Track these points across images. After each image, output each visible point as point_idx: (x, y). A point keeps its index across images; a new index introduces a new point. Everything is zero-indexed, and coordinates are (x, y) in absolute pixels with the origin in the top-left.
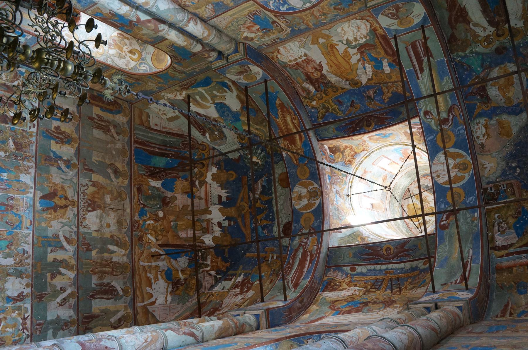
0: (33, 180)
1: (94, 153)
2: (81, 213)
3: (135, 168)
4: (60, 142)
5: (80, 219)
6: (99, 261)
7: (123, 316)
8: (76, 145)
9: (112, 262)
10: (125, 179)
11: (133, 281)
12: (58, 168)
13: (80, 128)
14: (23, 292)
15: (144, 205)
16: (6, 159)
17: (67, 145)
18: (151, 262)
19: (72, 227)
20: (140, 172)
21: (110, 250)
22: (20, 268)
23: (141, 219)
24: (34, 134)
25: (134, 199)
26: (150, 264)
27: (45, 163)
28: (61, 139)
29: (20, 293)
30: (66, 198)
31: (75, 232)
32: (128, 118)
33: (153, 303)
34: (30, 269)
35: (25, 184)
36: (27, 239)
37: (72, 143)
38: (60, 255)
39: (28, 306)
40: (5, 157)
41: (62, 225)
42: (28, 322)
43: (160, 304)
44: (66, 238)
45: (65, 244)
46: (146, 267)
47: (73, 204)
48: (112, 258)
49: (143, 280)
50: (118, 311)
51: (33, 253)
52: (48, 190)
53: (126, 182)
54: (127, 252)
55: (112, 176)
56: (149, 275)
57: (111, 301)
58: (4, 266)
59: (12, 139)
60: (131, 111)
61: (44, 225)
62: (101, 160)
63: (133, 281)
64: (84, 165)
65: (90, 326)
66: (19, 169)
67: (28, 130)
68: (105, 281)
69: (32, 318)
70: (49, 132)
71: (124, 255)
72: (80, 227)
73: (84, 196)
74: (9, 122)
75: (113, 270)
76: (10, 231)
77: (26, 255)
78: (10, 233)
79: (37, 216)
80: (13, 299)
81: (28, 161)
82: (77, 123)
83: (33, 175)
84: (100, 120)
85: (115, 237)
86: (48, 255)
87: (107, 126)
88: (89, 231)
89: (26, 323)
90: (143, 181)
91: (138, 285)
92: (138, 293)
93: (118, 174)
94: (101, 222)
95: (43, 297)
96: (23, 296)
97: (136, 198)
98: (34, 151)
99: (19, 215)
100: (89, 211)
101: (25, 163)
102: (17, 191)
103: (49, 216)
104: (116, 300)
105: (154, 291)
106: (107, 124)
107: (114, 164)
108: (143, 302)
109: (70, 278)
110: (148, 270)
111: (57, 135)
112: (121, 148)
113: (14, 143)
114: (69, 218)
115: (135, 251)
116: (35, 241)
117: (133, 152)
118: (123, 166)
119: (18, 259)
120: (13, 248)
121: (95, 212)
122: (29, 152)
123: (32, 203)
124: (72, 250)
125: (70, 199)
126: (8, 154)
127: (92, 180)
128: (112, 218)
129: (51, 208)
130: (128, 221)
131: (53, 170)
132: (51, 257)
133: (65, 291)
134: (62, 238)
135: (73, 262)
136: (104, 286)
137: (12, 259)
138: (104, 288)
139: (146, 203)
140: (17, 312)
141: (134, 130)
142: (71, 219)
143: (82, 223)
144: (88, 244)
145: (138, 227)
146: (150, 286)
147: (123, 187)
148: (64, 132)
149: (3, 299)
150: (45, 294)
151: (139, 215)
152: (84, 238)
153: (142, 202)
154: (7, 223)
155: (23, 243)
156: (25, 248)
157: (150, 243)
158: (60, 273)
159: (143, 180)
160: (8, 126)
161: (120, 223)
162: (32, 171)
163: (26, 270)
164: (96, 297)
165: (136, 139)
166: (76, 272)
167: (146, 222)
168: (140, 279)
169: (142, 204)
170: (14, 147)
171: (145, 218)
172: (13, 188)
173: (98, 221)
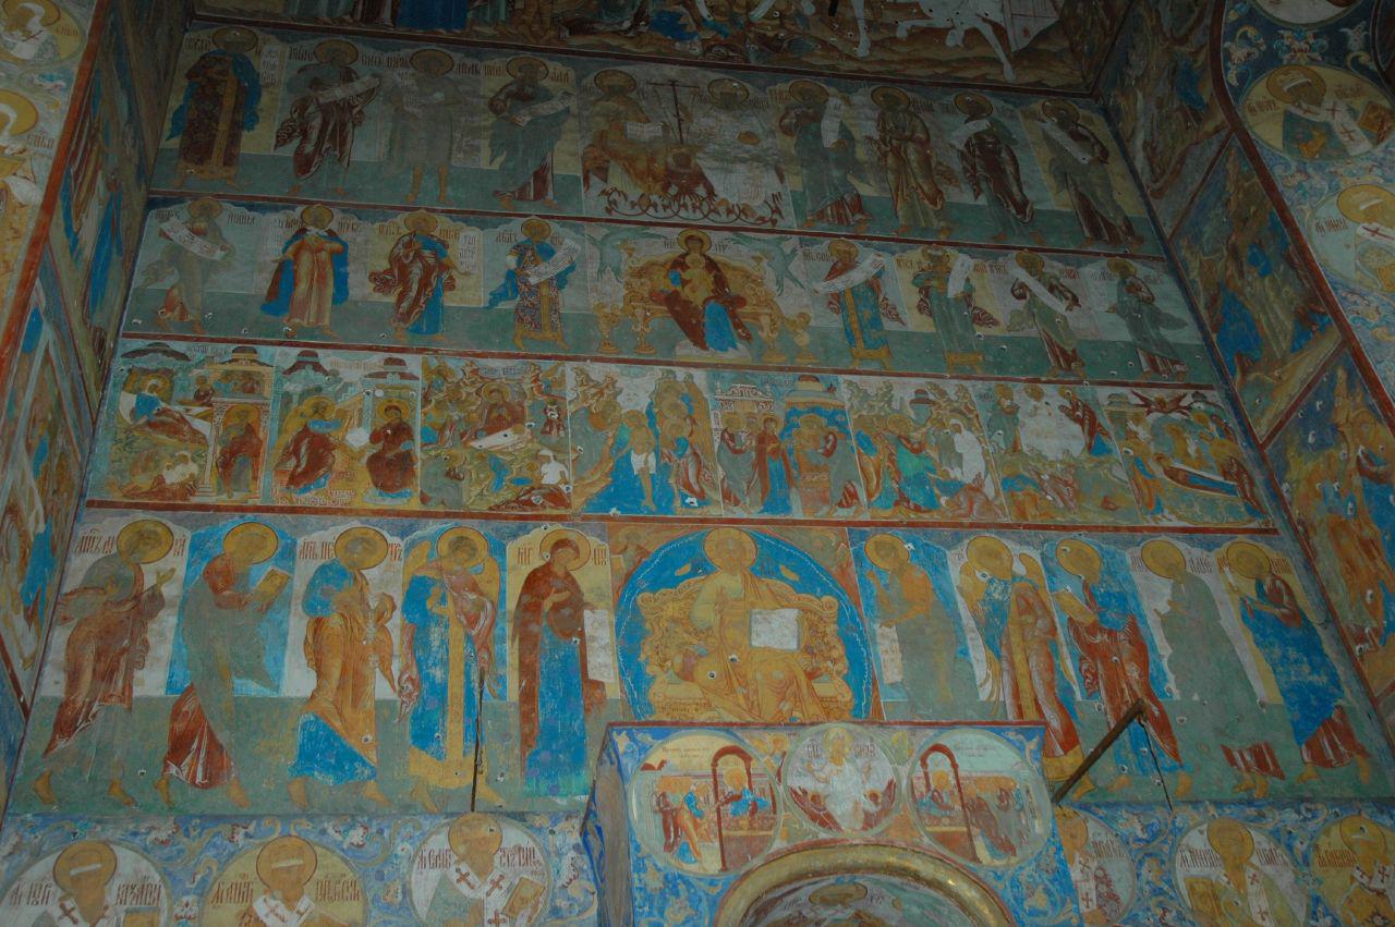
0: (635, 369)
1: (458, 160)
2: (724, 218)
3: (488, 31)
4: (445, 276)
5: (742, 224)
6: (891, 177)
7: (1062, 125)
8: (443, 223)
9: (883, 140)
10: (542, 69)
11: (931, 84)
12: (560, 287)
13: (358, 206)
14: (1062, 408)
15: (639, 16)
16: (572, 456)
17: (449, 251)
18: (855, 20)
19: (788, 251)
20: (503, 17)
21: (839, 142)
22: (984, 416)
23: (695, 34)
24: (434, 363)
25: (618, 48)
26: (861, 25)
27: (553, 328)
28: (427, 271)
29: (1068, 415)
30: (679, 263)
31: (801, 243)
32: (261, 35)
33: (997, 28)
34: (979, 384)
35: (658, 395)
36: (872, 392)
37: (436, 233)
38: (902, 290)
39: (1103, 393)
40: (562, 462)
41: (787, 282)
42: (1154, 394)
43: (1002, 10)
44: (834, 272)
45: (857, 276)
46: (877, 37)
47: (694, 240)
48: (870, 139)
49: (924, 54)
50: (1048, 139)
51: (917, 375)
52: (661, 320)
53: (555, 67)
54: (831, 90)
55: (544, 108)
56: (901, 33)
57: (1018, 154)
58: (987, 462)
59: (476, 437)
60: (224, 21)
61: (804, 339)
62: (484, 143)
63: (931, 84)
64: (522, 197)
65: (1119, 222)
66: (603, 415)
67: (419, 385)
68: (957, 166)
69: (1137, 385)
70: (409, 313)
71: (848, 102)
72: (781, 225)
73: (655, 206)
74: (403, 448)
75: (910, 139)
76: (860, 444)
77: (931, 397)
78: (866, 443)
79: (778, 360)
80: (1091, 434)
81: (561, 382)
82: (338, 215)
83: (614, 368)
84: (305, 134)
85: (786, 121)
86: (911, 327)
87: (325, 110)
88: (787, 199)
89: (1161, 403)
90: (539, 13)
91: (941, 70)
92: (970, 74)
93: (529, 90)
94: (744, 161)
95: (1064, 352)
96: (1075, 408)
97: (615, 42)
98: (510, 363)
99: (788, 415)
100: (711, 193)
101: (570, 396)
102: (694, 422)
103: (765, 320)
104: (1015, 142)
105: (957, 22)
106: (311, 109)
107: (492, 100)
108: (996, 62)
109: (976, 269)
110: (885, 33)
111: (415, 287)
112: (411, 71)
113: (491, 429)
114: (759, 260)
115: (820, 67)
116: (874, 367)
117: (419, 33)
118: (490, 71)
119: (953, 421)
120: (916, 436)
121: (707, 173)
122: (520, 383)
123: (727, 374)
124: (872, 256)
125: (679, 250)
126: (546, 452)
127: (580, 174)
128: (719, 126)
129: (734, 316)
130: (713, 76)
131: (570, 300)
132: (917, 323)
133: (1023, 286)
134: (839, 284)
135: (916, 255)
136: (974, 168)
137: (957, 438)
138: (980, 171)
139: (630, 13)
140: (1132, 426)
141: (316, 19)
142: (758, 254)
143: (762, 219)
144: (839, 204)
145: (727, 46)
146: (940, 34)
147: (579, 79)
148: (394, 259)
149: (1101, 463)
150: (1051, 344)
151: (681, 39)
152: (821, 215)
153: (627, 24)
154: (828, 453)
155: (889, 402)
156: (908, 399)
157: (782, 17)
158: (967, 297)
159: (533, 10)
160: (418, 453)
161: (728, 103)
162: (597, 371)
163: (984, 397)
164: (1018, 198)
165: (359, 17)
166: (949, 250)
167: (704, 20)
168: (919, 61)
169: (634, 26)
170: (509, 432)
171: (687, 19)
172: (686, 433)
173: (740, 167)
